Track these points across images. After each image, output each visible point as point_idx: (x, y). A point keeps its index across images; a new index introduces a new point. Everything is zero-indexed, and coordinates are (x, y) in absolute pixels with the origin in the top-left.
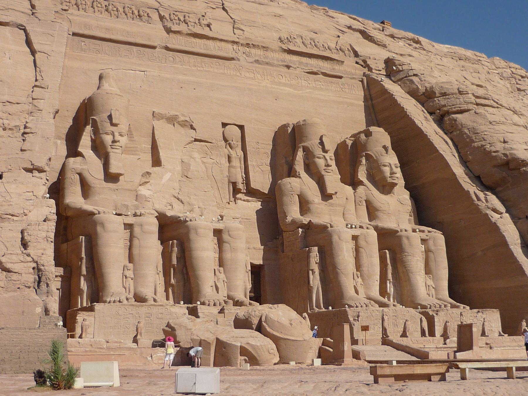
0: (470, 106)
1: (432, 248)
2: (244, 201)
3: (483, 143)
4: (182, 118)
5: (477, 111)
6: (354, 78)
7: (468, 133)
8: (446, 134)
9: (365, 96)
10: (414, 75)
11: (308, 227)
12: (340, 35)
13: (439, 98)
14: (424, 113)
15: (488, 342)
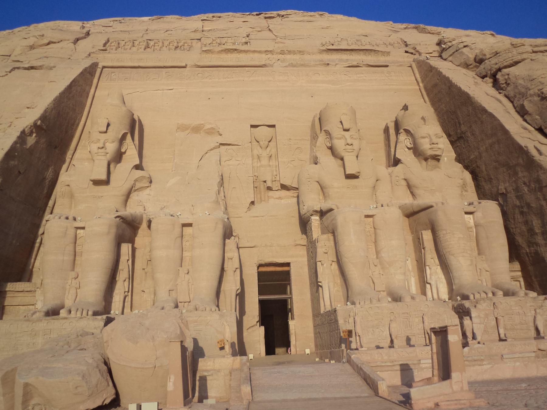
0: (525, 56)
1: (482, 222)
2: (277, 198)
3: (540, 87)
4: (208, 126)
5: (533, 58)
6: (401, 65)
7: (523, 83)
8: (500, 93)
9: (416, 80)
10: (465, 47)
11: (322, 213)
12: (394, 34)
13: (490, 59)
14: (475, 79)
15: (542, 347)
